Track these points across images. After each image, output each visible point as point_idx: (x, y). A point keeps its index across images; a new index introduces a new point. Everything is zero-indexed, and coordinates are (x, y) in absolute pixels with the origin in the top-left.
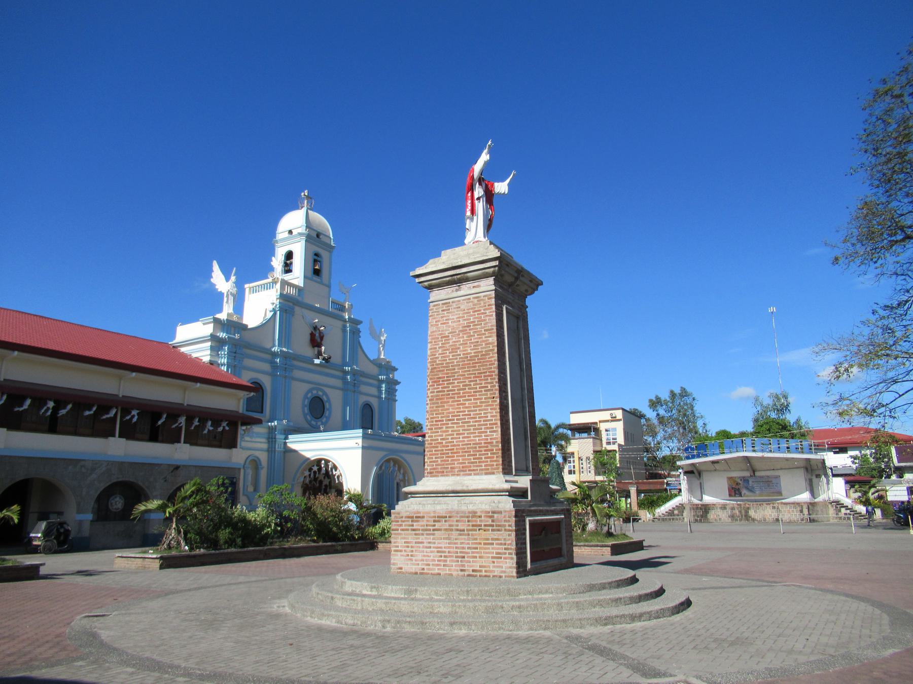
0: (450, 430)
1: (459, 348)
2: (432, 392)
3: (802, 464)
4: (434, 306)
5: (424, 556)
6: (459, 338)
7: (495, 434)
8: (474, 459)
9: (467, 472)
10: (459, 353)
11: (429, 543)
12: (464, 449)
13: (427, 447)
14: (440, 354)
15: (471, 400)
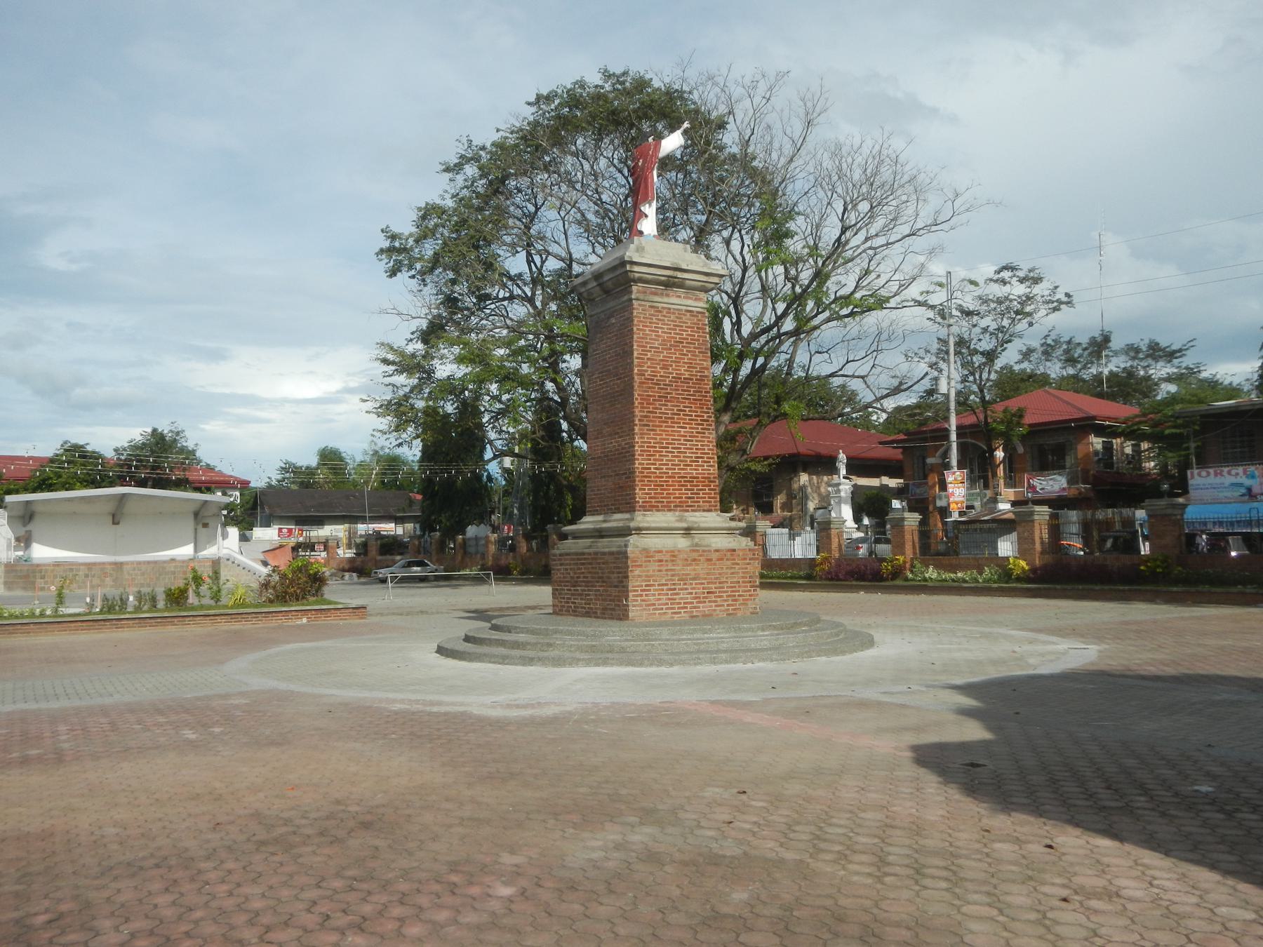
0: (665, 459)
1: (671, 366)
2: (641, 411)
3: (193, 507)
4: (640, 305)
5: (669, 599)
6: (670, 353)
7: (712, 469)
8: (692, 494)
9: (685, 508)
10: (670, 371)
11: (674, 584)
12: (681, 482)
13: (638, 476)
14: (648, 367)
15: (686, 428)
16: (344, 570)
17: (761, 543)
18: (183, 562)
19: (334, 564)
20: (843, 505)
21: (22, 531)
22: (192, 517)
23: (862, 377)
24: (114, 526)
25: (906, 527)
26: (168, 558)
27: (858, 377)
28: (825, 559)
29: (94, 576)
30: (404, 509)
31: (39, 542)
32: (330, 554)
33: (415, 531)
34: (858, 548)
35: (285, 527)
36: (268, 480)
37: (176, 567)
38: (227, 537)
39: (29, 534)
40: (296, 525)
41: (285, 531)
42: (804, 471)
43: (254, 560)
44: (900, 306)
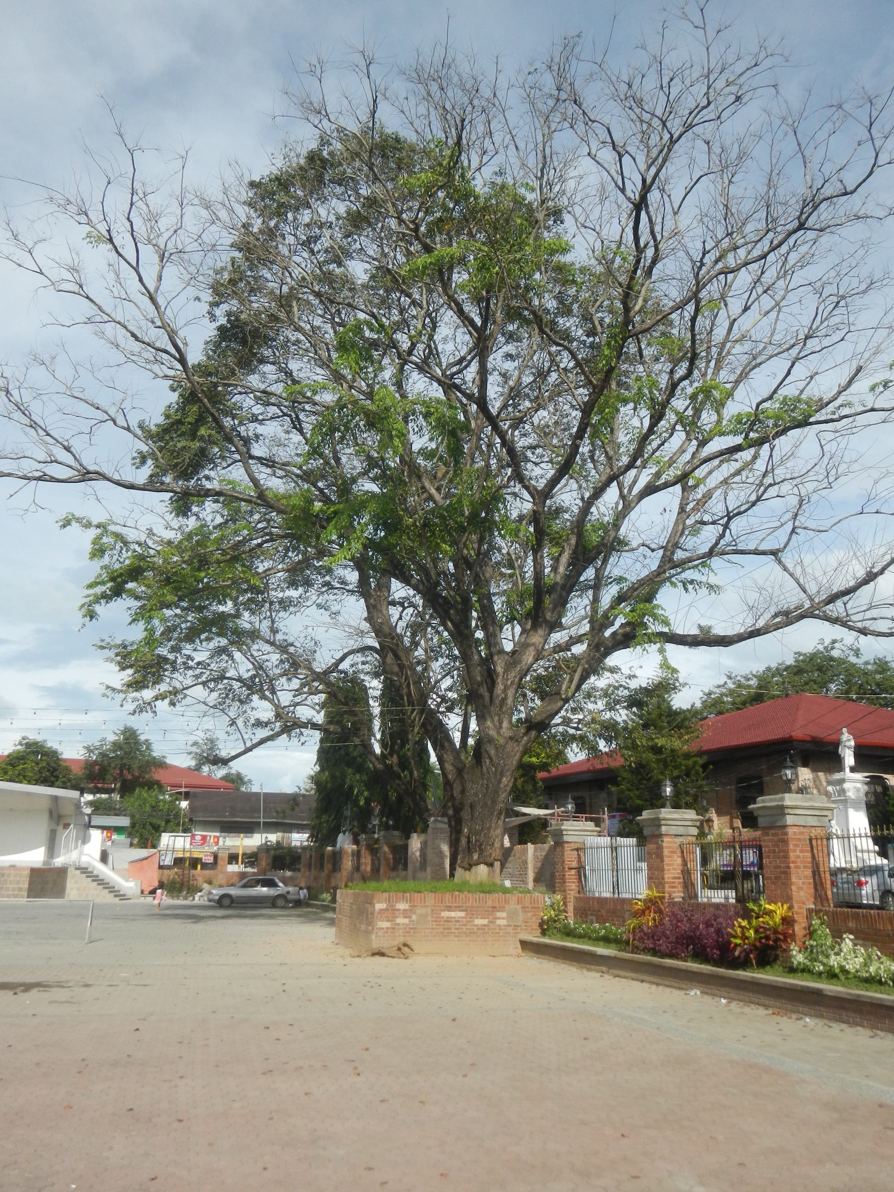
17: (574, 864)
20: (851, 812)
22: (45, 817)
23: (774, 553)
25: (790, 831)
26: (8, 864)
27: (763, 553)
28: (651, 903)
30: (284, 812)
33: (118, 830)
34: (860, 884)
35: (199, 833)
36: (297, 790)
38: (89, 841)
40: (221, 832)
41: (198, 838)
42: (805, 765)
44: (836, 417)
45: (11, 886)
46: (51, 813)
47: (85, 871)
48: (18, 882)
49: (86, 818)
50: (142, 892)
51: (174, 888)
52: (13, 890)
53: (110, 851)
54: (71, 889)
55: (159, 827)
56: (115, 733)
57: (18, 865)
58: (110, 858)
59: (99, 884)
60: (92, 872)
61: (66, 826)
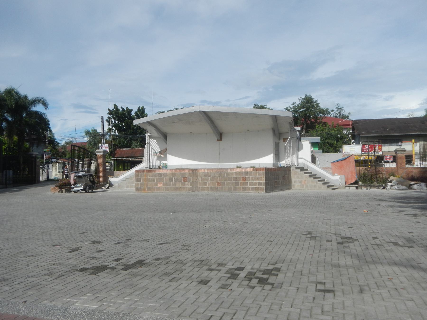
16: (413, 179)
18: (243, 169)
19: (402, 173)
21: (164, 148)
24: (219, 142)
29: (176, 180)
31: (171, 154)
32: (399, 164)
37: (237, 174)
38: (302, 149)
39: (166, 149)
41: (367, 147)
43: (324, 169)
45: (253, 182)
46: (274, 131)
47: (302, 169)
48: (258, 179)
49: (298, 133)
50: (346, 183)
51: (366, 180)
52: (255, 184)
53: (316, 155)
54: (295, 182)
55: (333, 144)
56: (300, 100)
57: (257, 166)
58: (317, 160)
59: (314, 178)
60: (307, 170)
61: (285, 140)
